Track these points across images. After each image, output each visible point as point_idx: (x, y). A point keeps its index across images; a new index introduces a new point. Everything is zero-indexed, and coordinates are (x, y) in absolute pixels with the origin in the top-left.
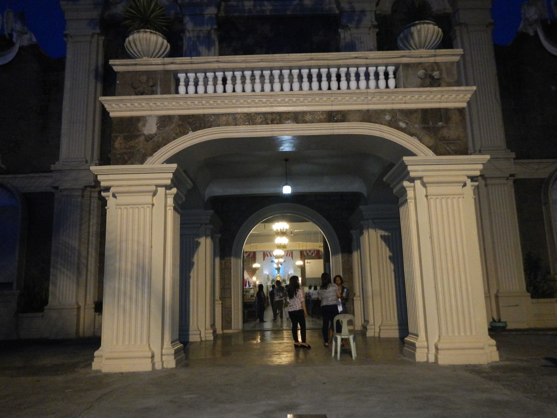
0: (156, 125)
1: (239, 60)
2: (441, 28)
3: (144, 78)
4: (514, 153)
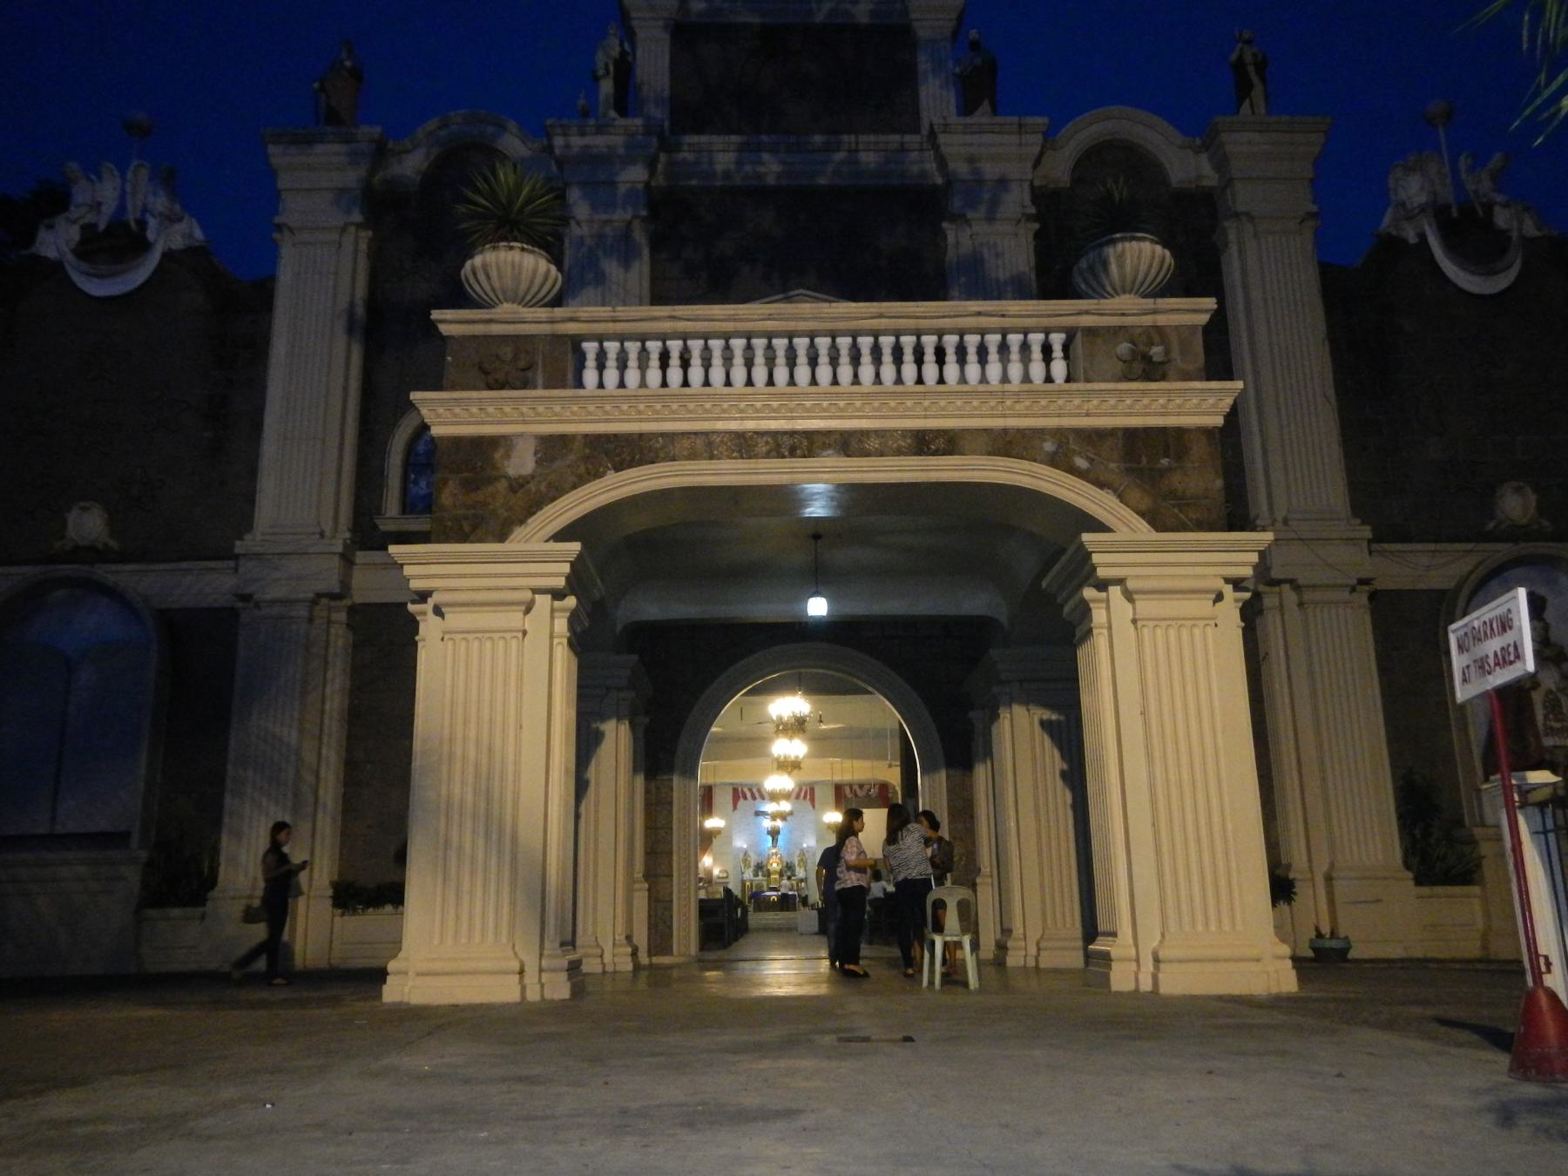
1: (718, 314)
2: (1169, 249)
4: (1368, 528)
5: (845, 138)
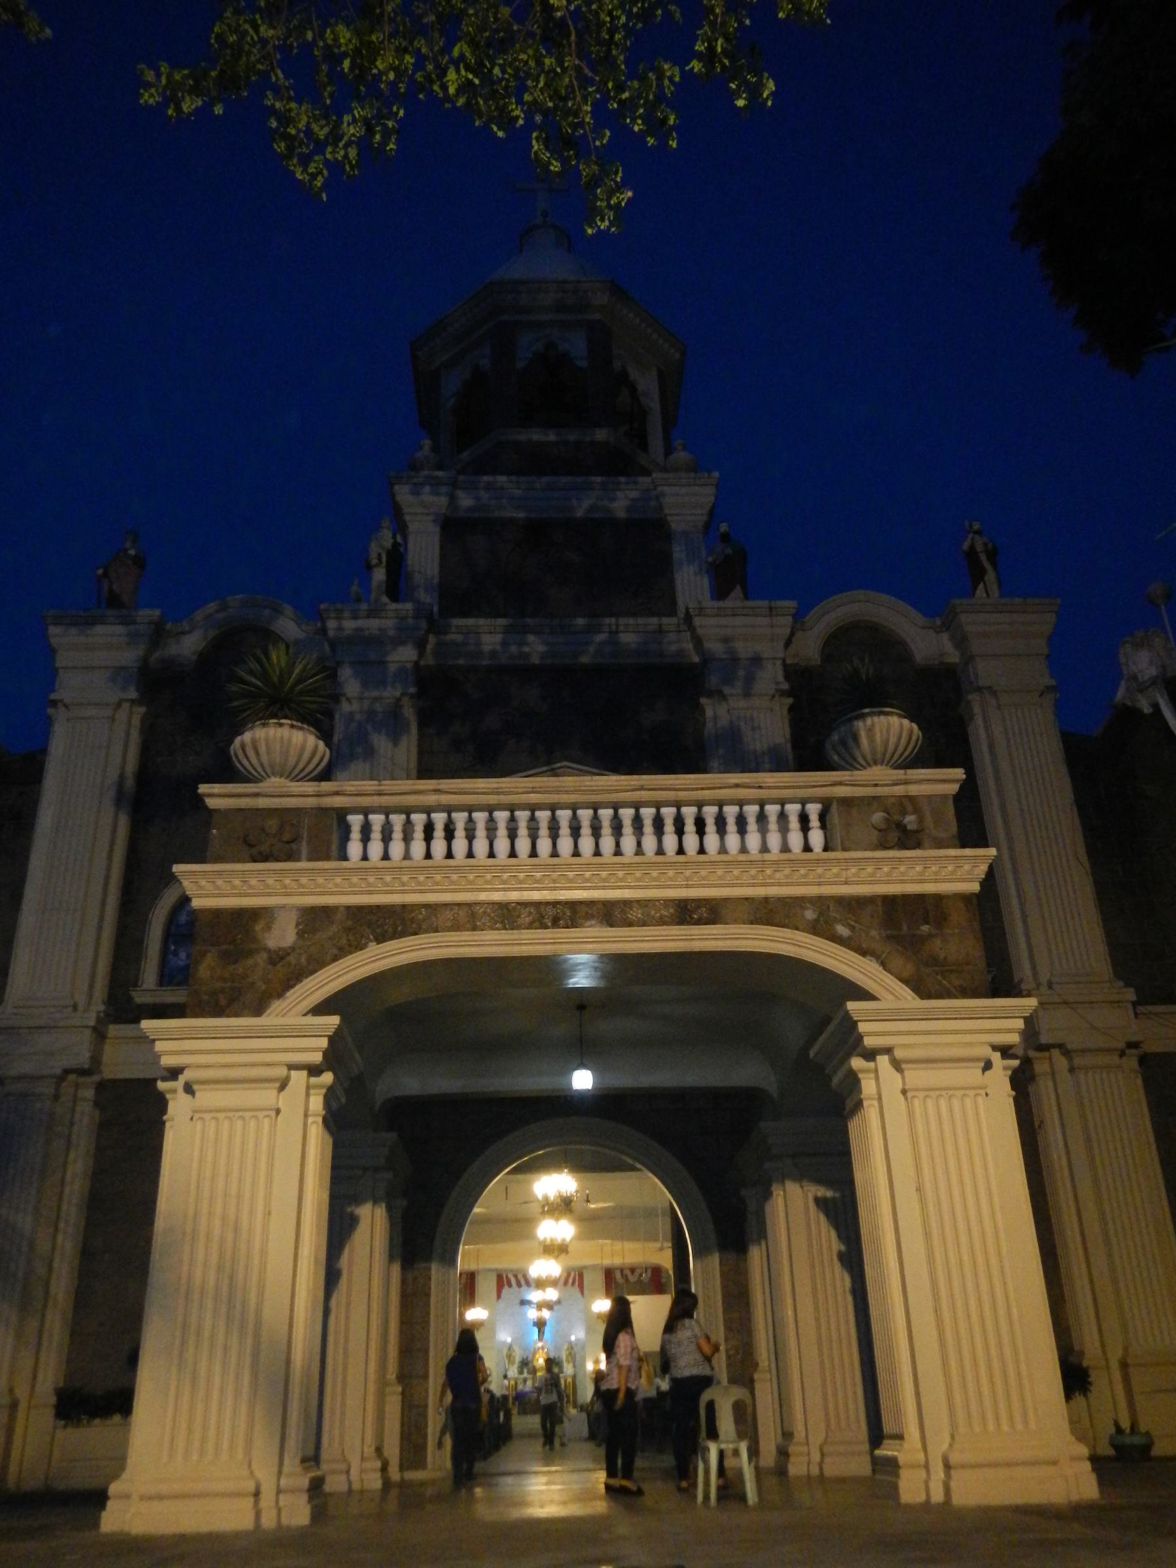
0: (296, 928)
1: (482, 787)
2: (917, 724)
3: (272, 824)
4: (1132, 990)
5: (607, 620)
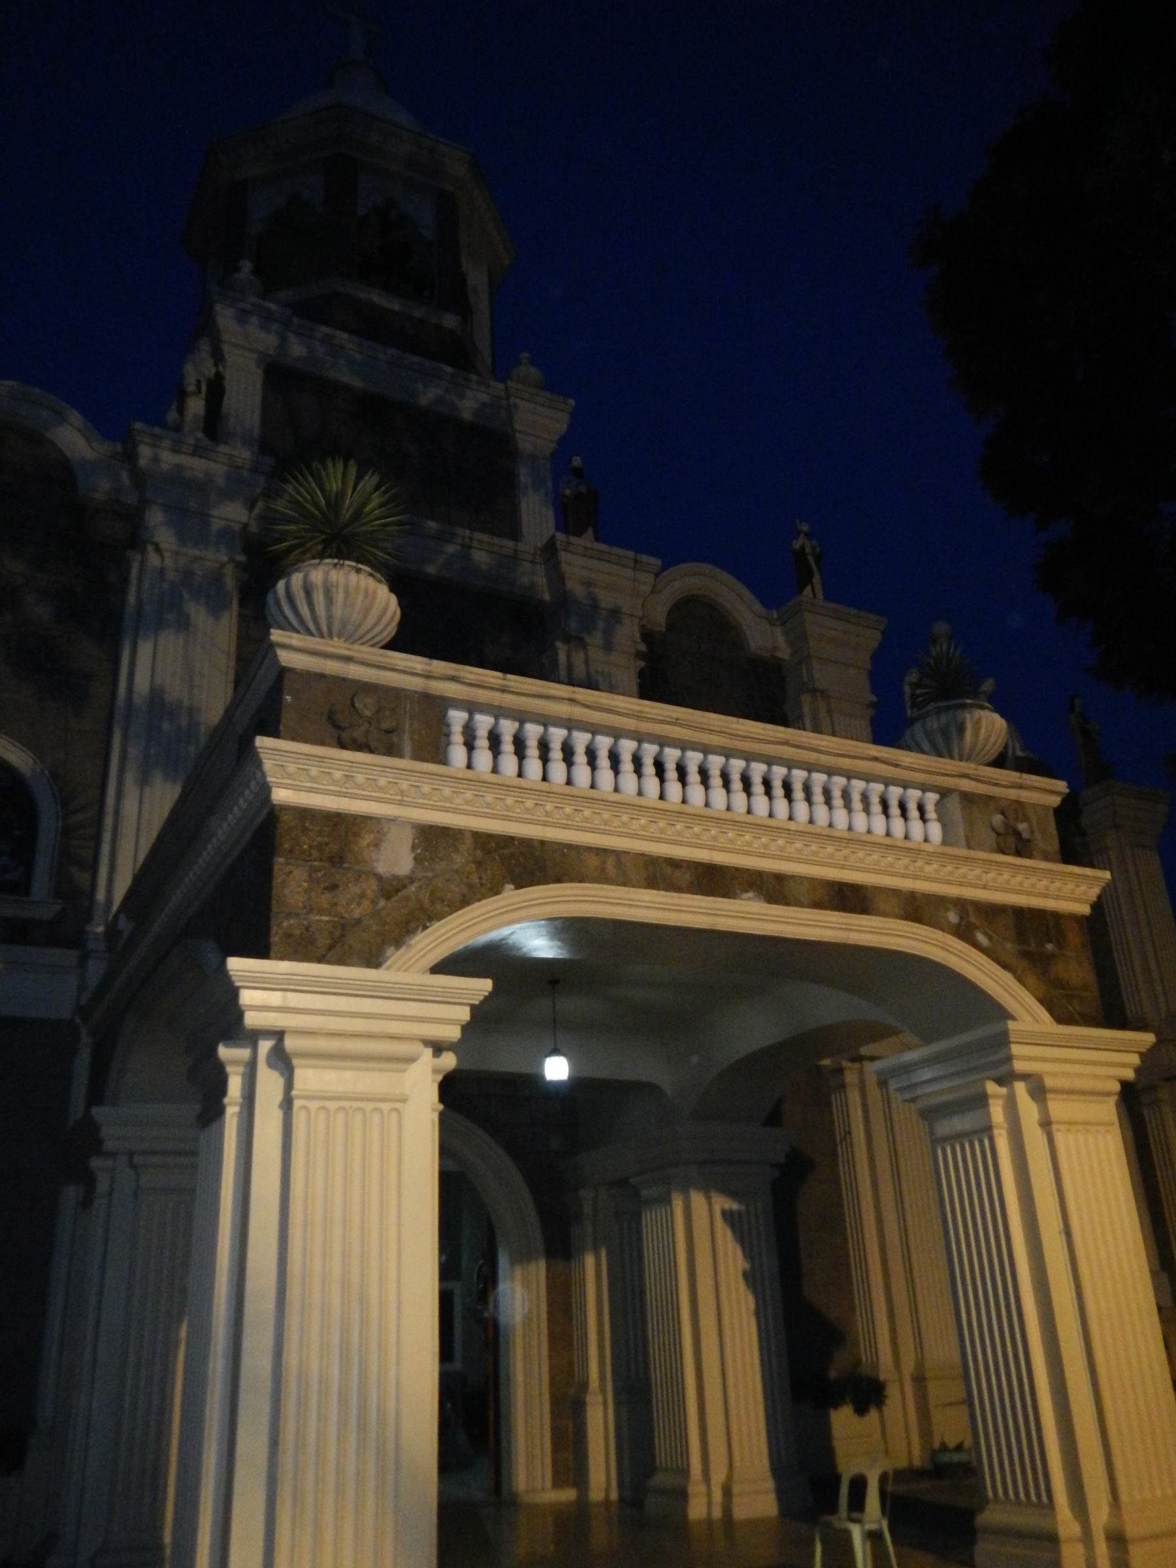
3: (366, 705)
5: (460, 531)
